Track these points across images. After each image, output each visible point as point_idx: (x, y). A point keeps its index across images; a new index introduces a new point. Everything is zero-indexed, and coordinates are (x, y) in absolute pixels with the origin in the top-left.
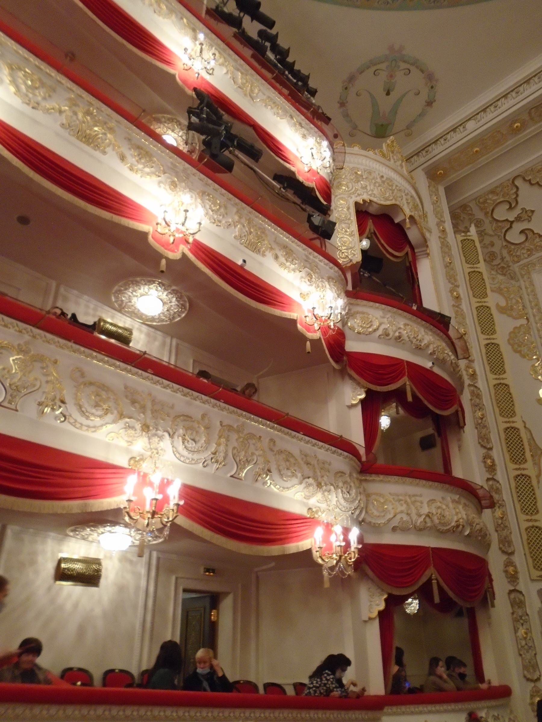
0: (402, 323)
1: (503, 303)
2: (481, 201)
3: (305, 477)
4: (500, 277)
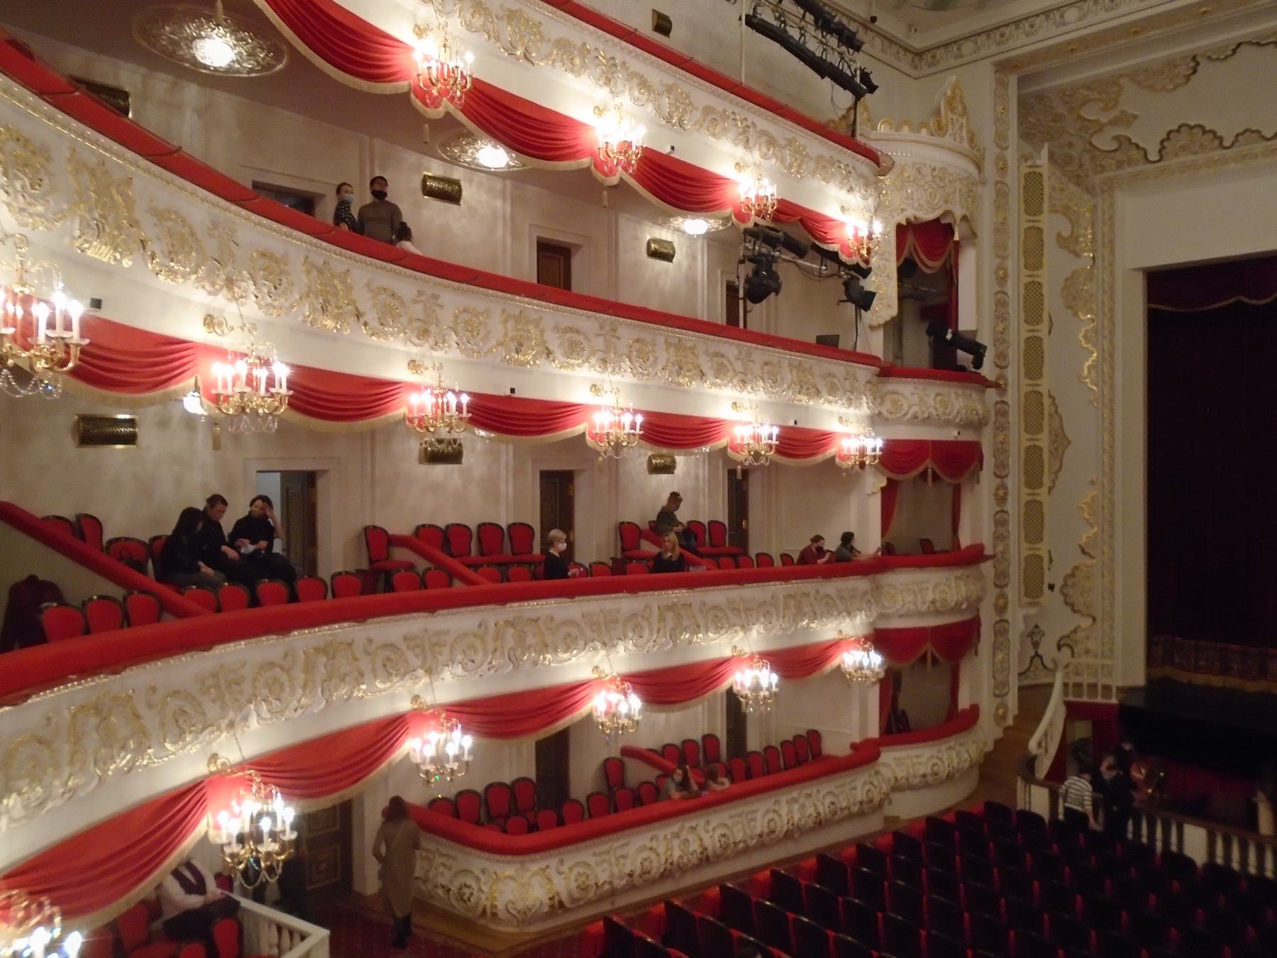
0: (933, 395)
1: (1066, 233)
2: (1067, 95)
3: (840, 613)
4: (1072, 187)
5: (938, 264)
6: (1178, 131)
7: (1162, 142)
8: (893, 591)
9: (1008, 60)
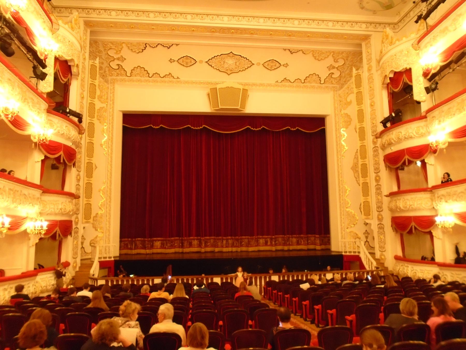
0: (65, 126)
2: (105, 44)
4: (101, 79)
5: (65, 80)
6: (137, 68)
7: (132, 70)
8: (45, 203)
9: (90, 22)
